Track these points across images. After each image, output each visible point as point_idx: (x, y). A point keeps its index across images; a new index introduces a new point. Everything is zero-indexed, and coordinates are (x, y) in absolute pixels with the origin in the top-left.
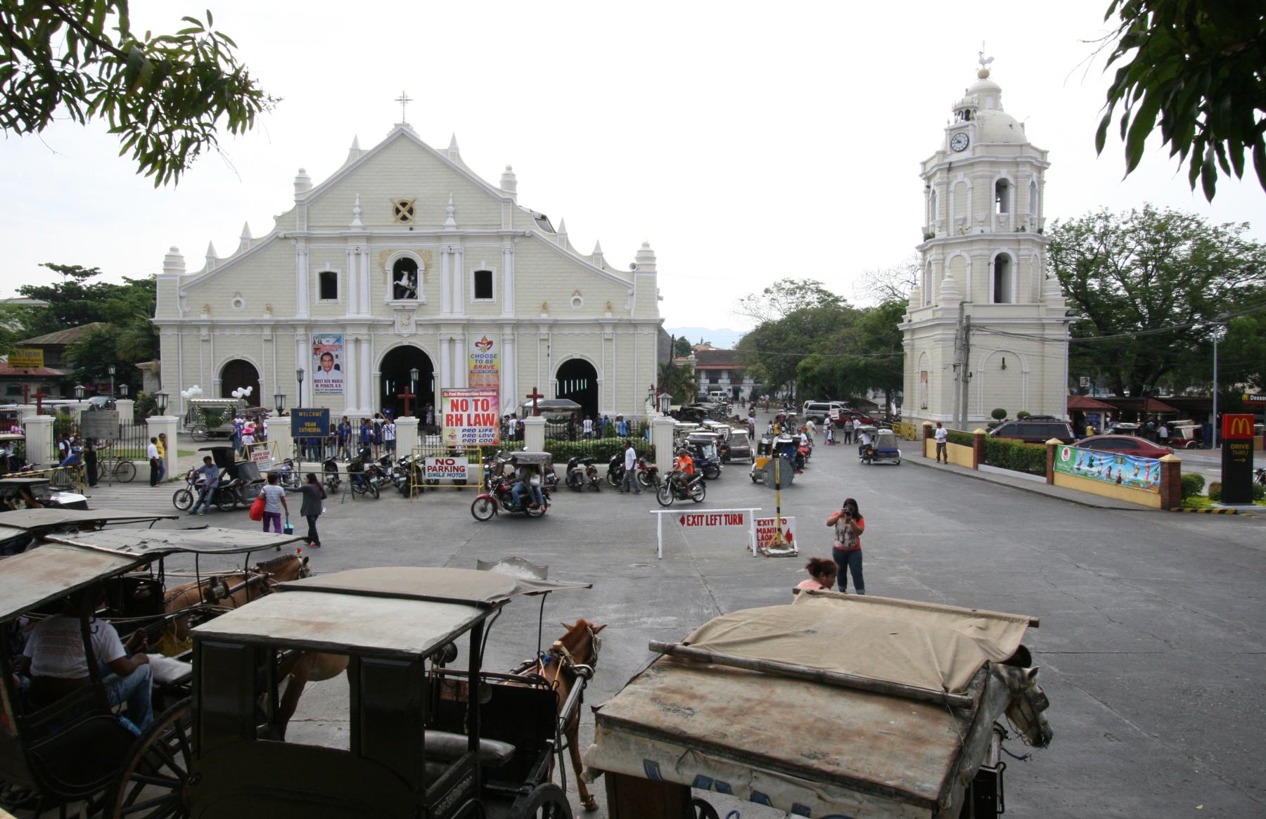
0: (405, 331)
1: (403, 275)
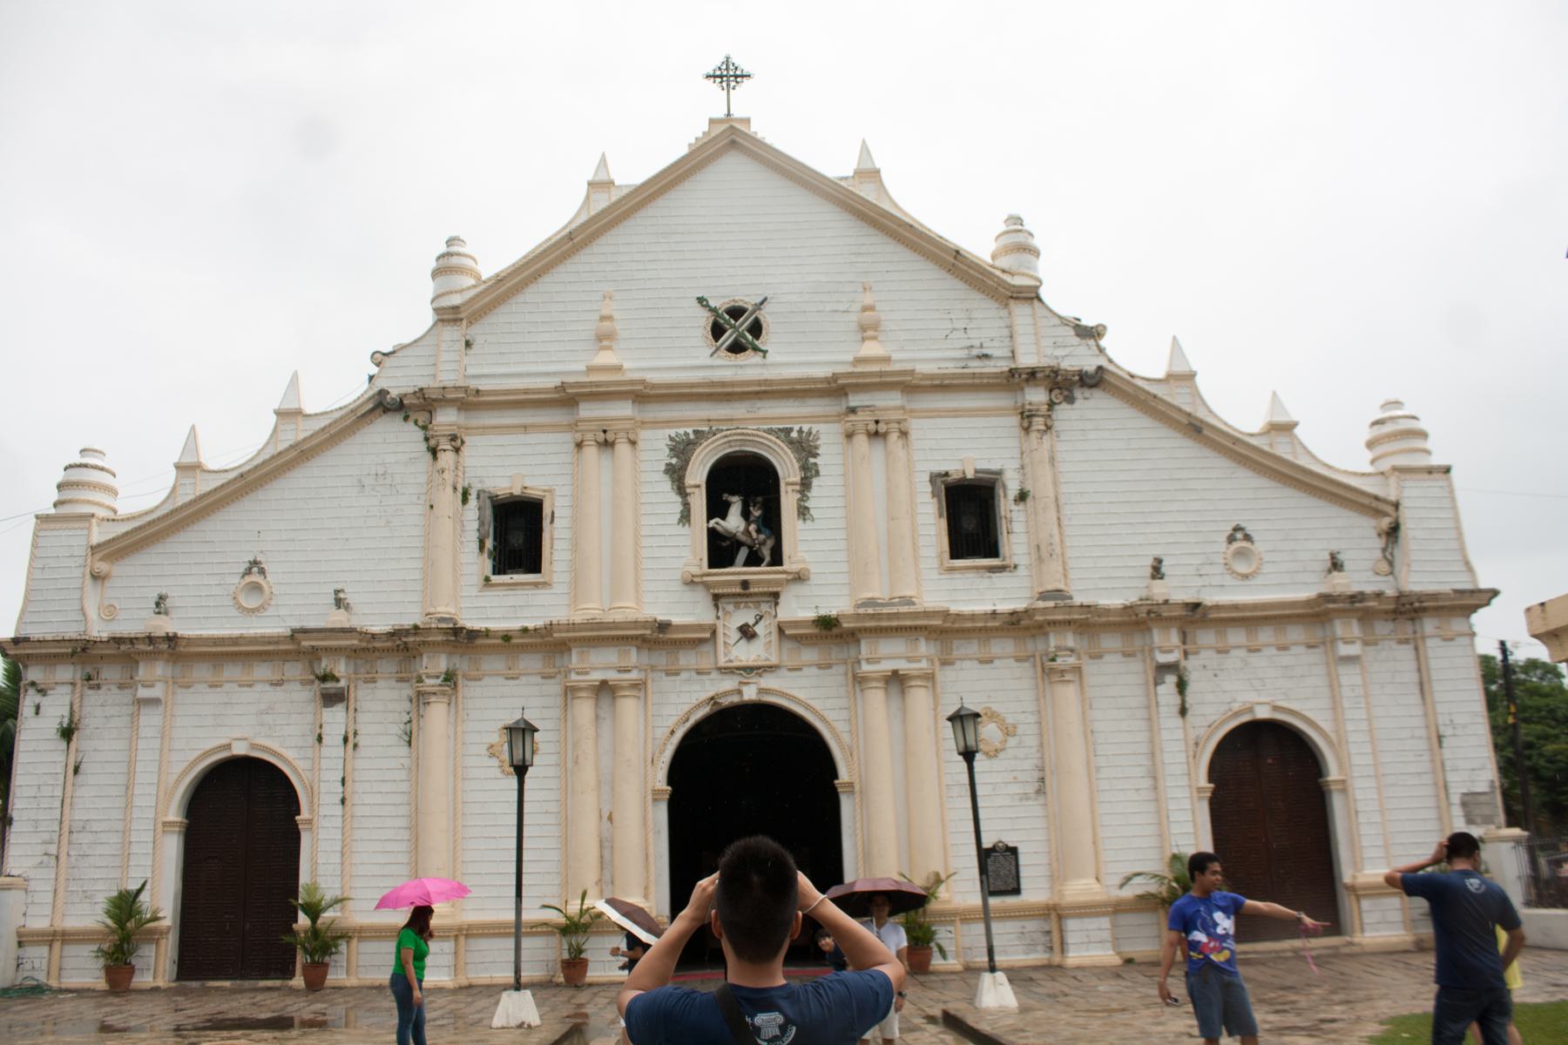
0: (747, 653)
1: (728, 505)
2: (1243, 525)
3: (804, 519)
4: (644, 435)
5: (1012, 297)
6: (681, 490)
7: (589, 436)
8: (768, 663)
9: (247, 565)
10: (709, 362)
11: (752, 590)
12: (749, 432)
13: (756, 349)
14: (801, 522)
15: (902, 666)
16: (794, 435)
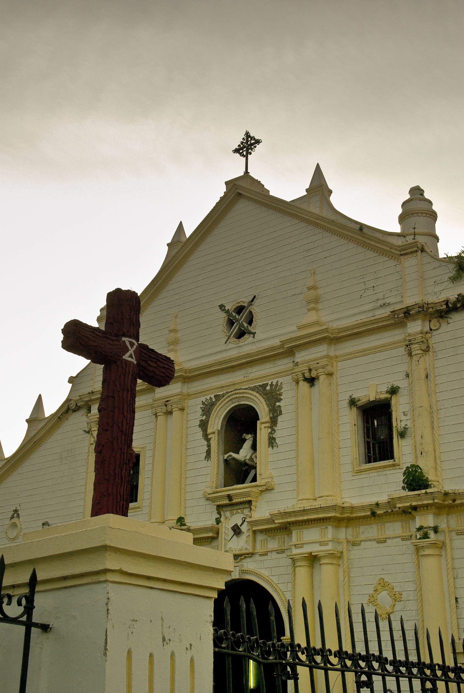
1: (245, 440)
3: (273, 447)
4: (191, 402)
5: (401, 255)
6: (206, 437)
7: (158, 410)
8: (246, 551)
9: (13, 513)
10: (225, 347)
11: (234, 501)
12: (240, 391)
13: (250, 333)
14: (271, 448)
15: (315, 549)
16: (268, 388)
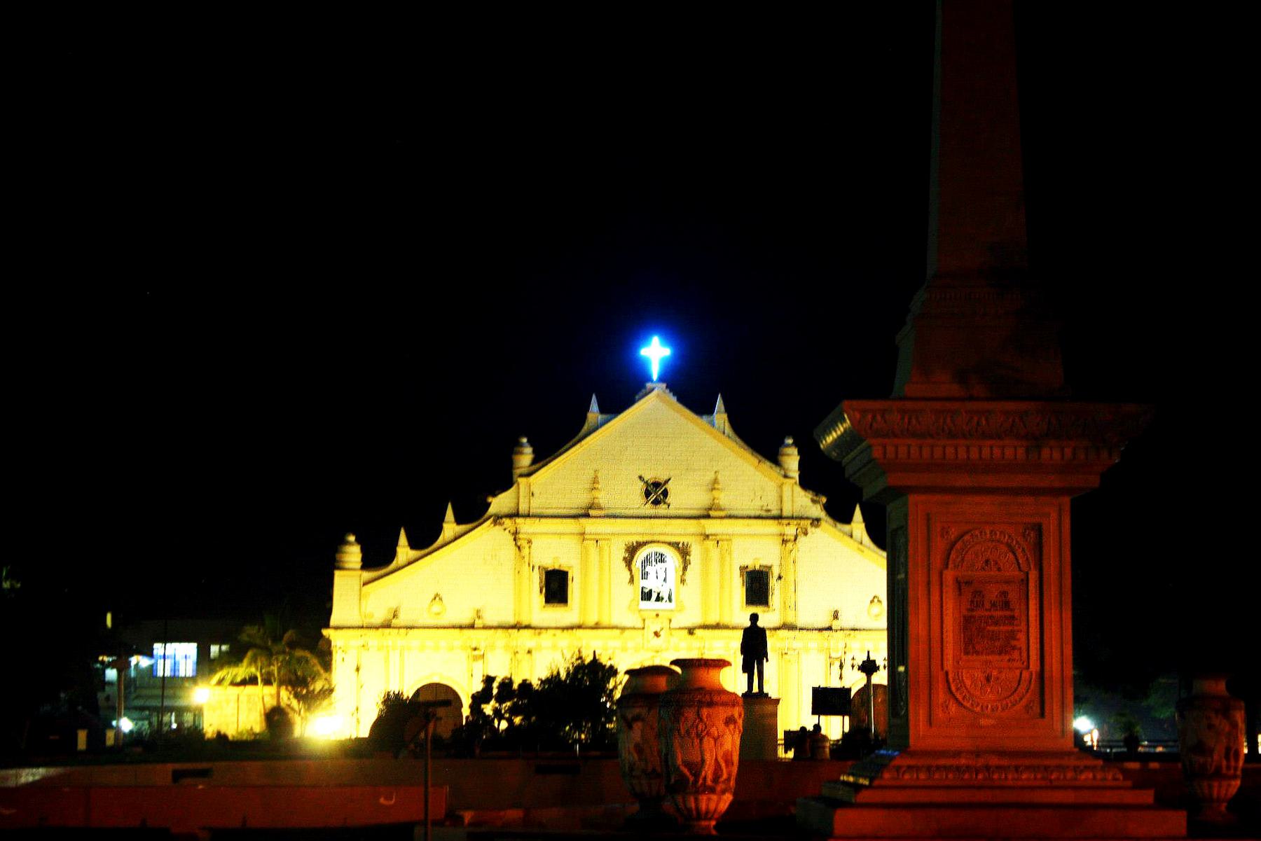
2: (877, 595)
13: (665, 503)
16: (680, 545)
